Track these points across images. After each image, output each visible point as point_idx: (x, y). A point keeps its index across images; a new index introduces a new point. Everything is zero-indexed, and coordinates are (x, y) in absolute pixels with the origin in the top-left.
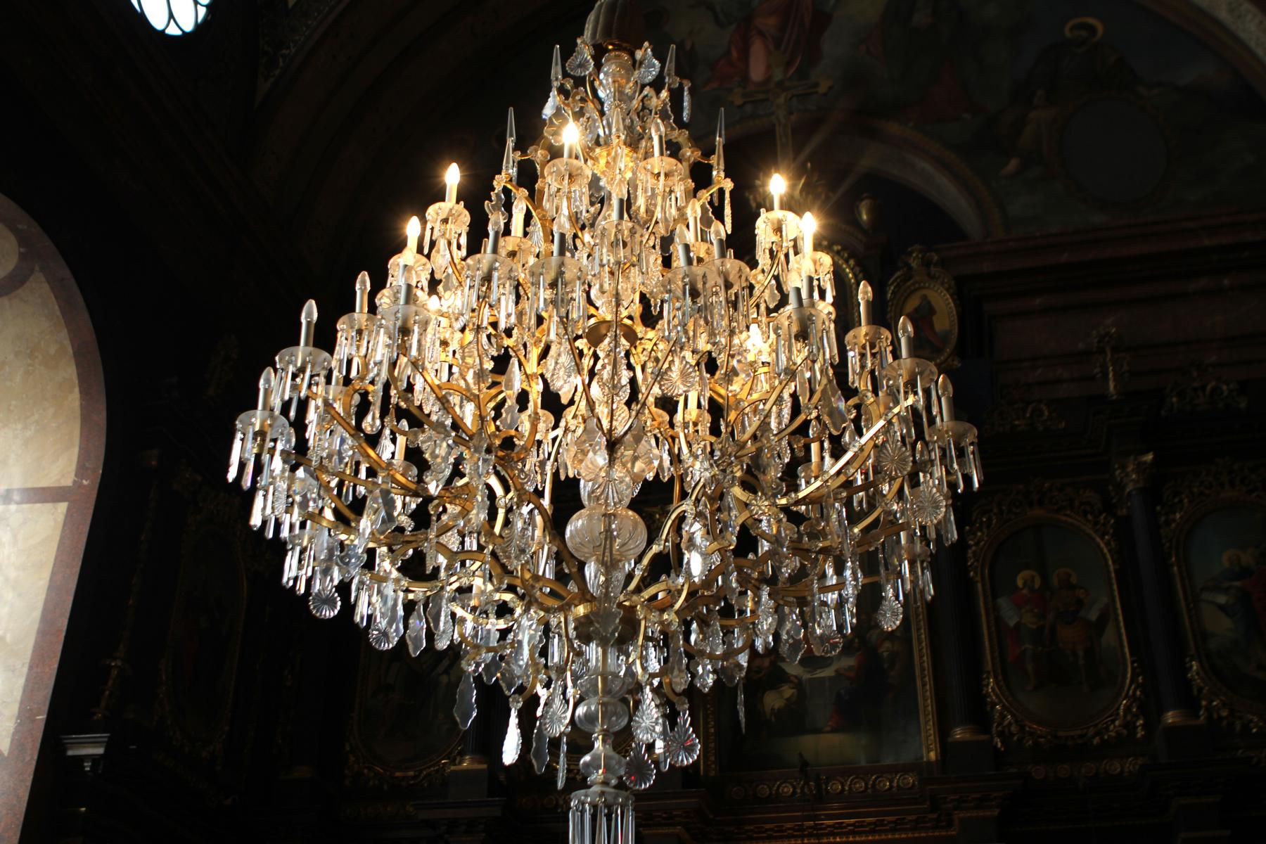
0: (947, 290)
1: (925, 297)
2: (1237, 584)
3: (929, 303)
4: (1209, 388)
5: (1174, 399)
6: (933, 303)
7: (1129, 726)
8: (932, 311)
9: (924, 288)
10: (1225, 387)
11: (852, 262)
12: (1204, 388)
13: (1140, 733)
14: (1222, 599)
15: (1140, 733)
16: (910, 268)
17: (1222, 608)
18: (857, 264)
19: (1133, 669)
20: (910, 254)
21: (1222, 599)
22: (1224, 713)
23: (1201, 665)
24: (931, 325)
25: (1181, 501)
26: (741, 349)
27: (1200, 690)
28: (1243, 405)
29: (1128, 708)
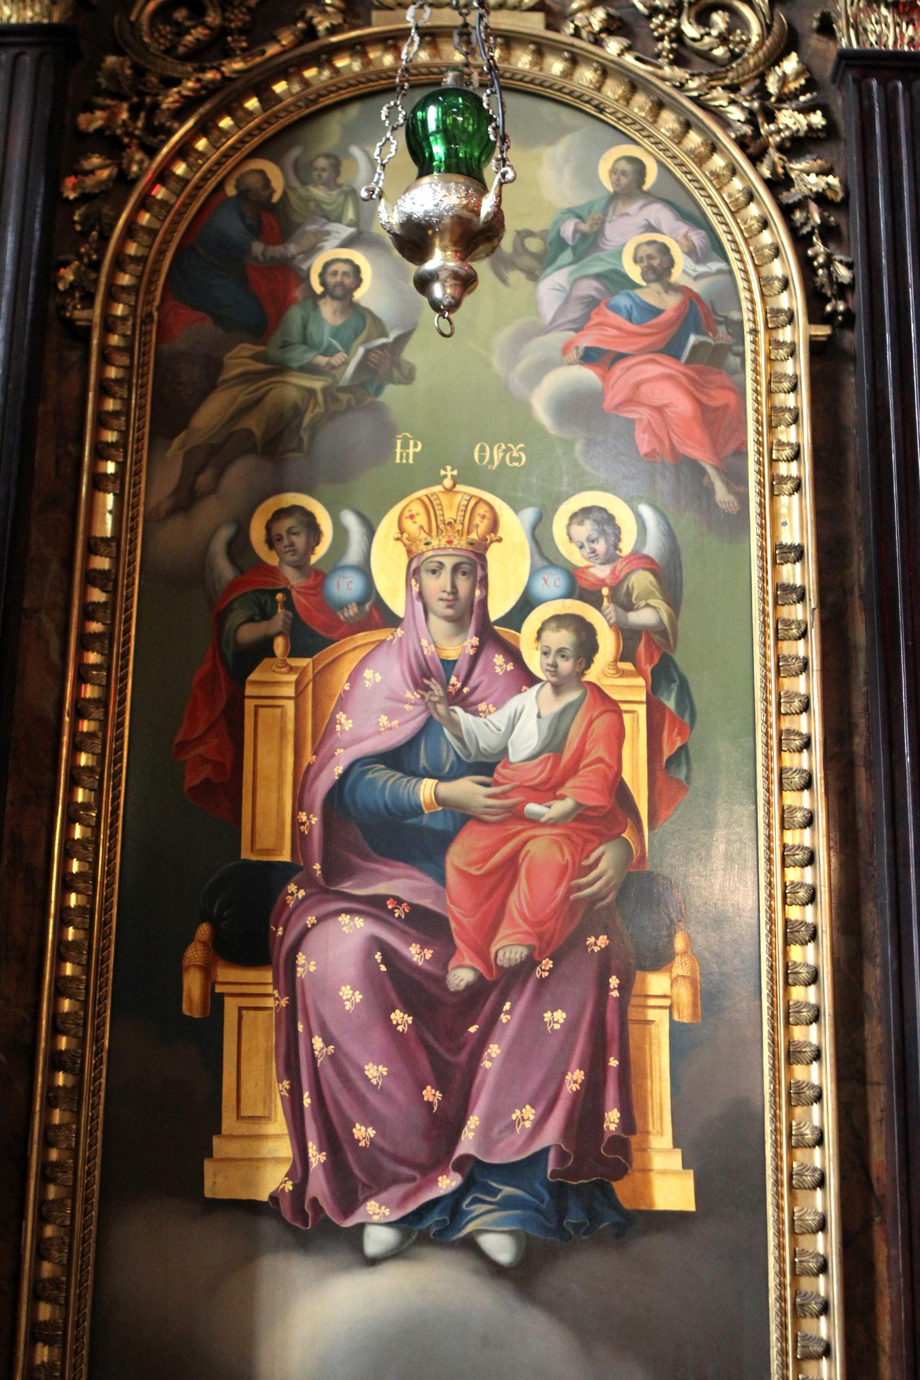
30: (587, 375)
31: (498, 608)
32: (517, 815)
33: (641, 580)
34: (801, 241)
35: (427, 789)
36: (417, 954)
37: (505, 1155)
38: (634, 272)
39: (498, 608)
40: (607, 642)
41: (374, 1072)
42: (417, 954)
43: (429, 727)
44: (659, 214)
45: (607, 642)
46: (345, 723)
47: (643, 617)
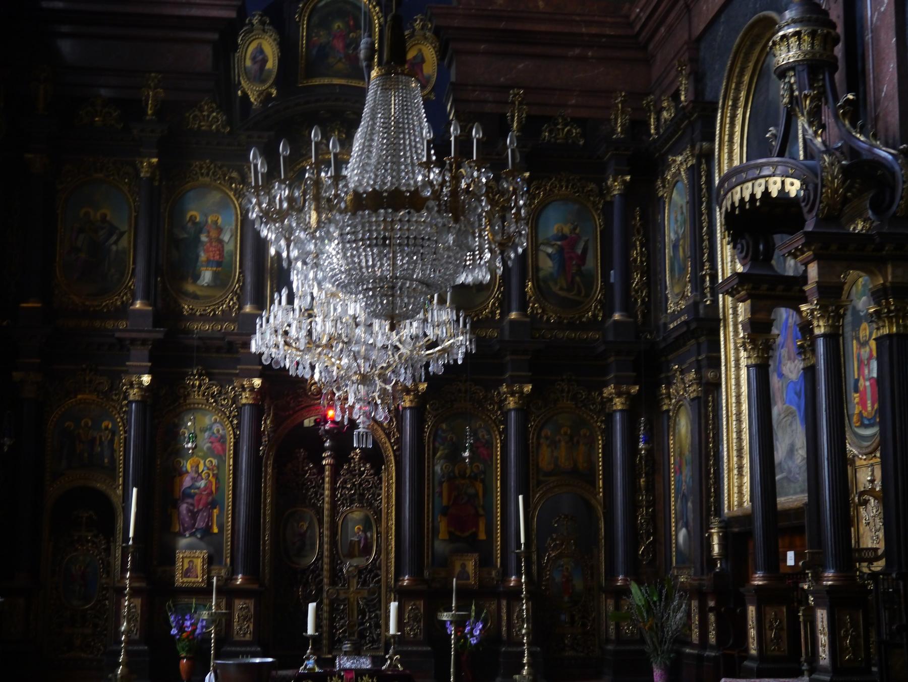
0: (434, 48)
1: (420, 50)
2: (559, 243)
3: (422, 54)
4: (566, 130)
5: (547, 134)
6: (424, 55)
7: (493, 312)
8: (423, 61)
9: (420, 44)
10: (574, 131)
11: (377, 9)
12: (563, 129)
13: (498, 317)
14: (550, 250)
15: (498, 317)
16: (414, 30)
17: (549, 255)
18: (381, 10)
19: (499, 283)
20: (416, 20)
21: (550, 250)
22: (540, 311)
23: (533, 284)
24: (422, 70)
25: (539, 193)
26: (421, 315)
27: (530, 297)
28: (581, 143)
29: (494, 304)
30: (209, 445)
31: (200, 471)
32: (201, 494)
33: (215, 468)
34: (233, 429)
35: (192, 491)
36: (191, 508)
37: (200, 527)
38: (215, 432)
39: (200, 471)
40: (211, 475)
41: (187, 519)
42: (191, 508)
43: (193, 484)
44: (218, 425)
45: (211, 475)
46: (184, 484)
47: (215, 472)
